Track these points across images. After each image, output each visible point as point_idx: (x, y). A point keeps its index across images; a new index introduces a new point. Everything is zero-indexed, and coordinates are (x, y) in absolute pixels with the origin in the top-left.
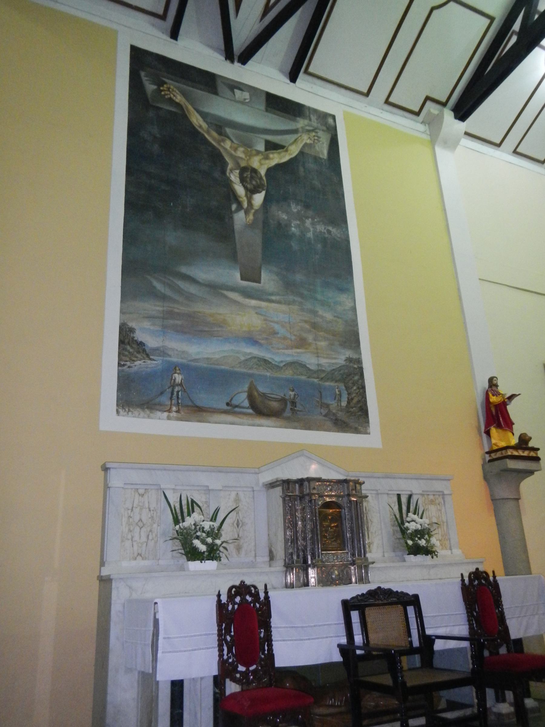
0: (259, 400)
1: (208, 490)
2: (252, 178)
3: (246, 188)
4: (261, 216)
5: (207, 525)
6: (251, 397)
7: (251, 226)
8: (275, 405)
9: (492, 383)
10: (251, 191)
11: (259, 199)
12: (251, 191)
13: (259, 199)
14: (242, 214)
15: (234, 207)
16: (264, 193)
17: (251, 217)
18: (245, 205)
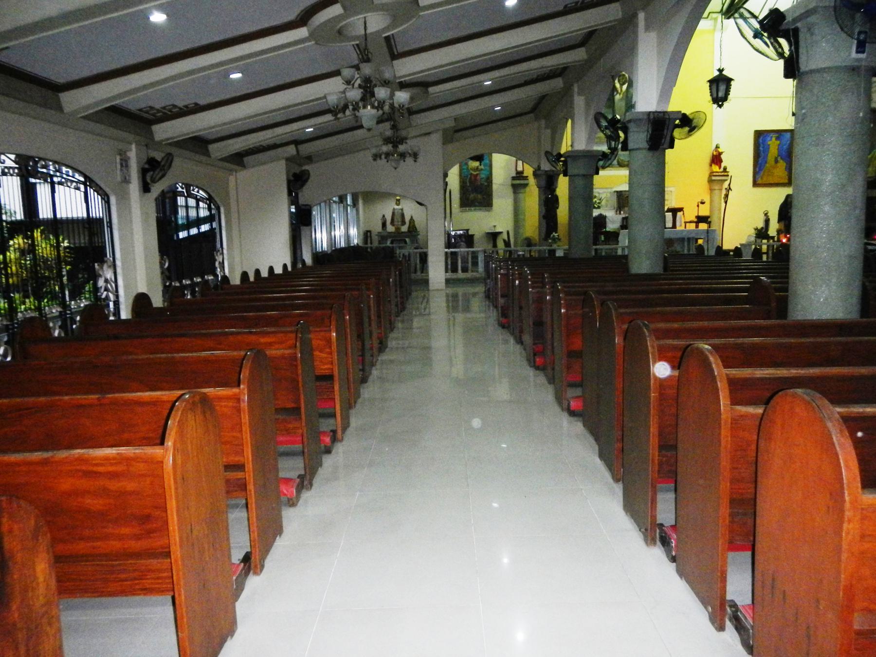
0: (620, 161)
1: (599, 193)
2: (623, 79)
3: (620, 84)
4: (625, 94)
5: (598, 201)
6: (618, 162)
7: (621, 100)
8: (626, 163)
9: (717, 147)
10: (621, 85)
11: (625, 87)
12: (621, 85)
13: (625, 87)
14: (618, 95)
15: (615, 93)
16: (627, 84)
17: (621, 96)
18: (619, 91)
